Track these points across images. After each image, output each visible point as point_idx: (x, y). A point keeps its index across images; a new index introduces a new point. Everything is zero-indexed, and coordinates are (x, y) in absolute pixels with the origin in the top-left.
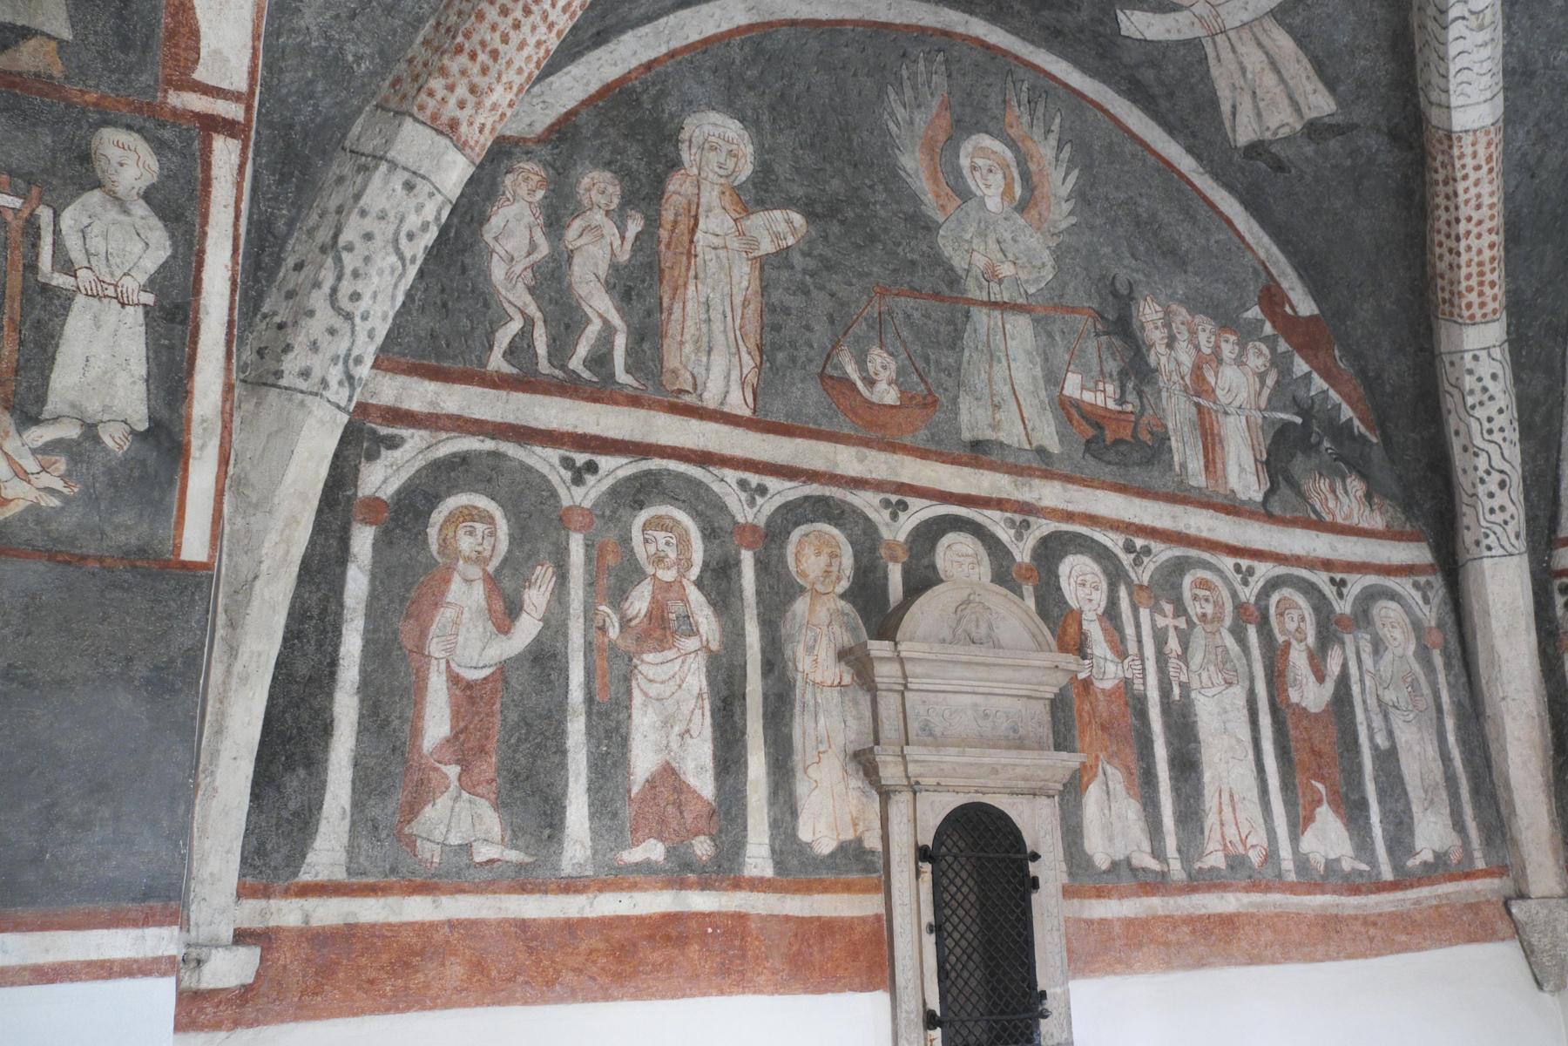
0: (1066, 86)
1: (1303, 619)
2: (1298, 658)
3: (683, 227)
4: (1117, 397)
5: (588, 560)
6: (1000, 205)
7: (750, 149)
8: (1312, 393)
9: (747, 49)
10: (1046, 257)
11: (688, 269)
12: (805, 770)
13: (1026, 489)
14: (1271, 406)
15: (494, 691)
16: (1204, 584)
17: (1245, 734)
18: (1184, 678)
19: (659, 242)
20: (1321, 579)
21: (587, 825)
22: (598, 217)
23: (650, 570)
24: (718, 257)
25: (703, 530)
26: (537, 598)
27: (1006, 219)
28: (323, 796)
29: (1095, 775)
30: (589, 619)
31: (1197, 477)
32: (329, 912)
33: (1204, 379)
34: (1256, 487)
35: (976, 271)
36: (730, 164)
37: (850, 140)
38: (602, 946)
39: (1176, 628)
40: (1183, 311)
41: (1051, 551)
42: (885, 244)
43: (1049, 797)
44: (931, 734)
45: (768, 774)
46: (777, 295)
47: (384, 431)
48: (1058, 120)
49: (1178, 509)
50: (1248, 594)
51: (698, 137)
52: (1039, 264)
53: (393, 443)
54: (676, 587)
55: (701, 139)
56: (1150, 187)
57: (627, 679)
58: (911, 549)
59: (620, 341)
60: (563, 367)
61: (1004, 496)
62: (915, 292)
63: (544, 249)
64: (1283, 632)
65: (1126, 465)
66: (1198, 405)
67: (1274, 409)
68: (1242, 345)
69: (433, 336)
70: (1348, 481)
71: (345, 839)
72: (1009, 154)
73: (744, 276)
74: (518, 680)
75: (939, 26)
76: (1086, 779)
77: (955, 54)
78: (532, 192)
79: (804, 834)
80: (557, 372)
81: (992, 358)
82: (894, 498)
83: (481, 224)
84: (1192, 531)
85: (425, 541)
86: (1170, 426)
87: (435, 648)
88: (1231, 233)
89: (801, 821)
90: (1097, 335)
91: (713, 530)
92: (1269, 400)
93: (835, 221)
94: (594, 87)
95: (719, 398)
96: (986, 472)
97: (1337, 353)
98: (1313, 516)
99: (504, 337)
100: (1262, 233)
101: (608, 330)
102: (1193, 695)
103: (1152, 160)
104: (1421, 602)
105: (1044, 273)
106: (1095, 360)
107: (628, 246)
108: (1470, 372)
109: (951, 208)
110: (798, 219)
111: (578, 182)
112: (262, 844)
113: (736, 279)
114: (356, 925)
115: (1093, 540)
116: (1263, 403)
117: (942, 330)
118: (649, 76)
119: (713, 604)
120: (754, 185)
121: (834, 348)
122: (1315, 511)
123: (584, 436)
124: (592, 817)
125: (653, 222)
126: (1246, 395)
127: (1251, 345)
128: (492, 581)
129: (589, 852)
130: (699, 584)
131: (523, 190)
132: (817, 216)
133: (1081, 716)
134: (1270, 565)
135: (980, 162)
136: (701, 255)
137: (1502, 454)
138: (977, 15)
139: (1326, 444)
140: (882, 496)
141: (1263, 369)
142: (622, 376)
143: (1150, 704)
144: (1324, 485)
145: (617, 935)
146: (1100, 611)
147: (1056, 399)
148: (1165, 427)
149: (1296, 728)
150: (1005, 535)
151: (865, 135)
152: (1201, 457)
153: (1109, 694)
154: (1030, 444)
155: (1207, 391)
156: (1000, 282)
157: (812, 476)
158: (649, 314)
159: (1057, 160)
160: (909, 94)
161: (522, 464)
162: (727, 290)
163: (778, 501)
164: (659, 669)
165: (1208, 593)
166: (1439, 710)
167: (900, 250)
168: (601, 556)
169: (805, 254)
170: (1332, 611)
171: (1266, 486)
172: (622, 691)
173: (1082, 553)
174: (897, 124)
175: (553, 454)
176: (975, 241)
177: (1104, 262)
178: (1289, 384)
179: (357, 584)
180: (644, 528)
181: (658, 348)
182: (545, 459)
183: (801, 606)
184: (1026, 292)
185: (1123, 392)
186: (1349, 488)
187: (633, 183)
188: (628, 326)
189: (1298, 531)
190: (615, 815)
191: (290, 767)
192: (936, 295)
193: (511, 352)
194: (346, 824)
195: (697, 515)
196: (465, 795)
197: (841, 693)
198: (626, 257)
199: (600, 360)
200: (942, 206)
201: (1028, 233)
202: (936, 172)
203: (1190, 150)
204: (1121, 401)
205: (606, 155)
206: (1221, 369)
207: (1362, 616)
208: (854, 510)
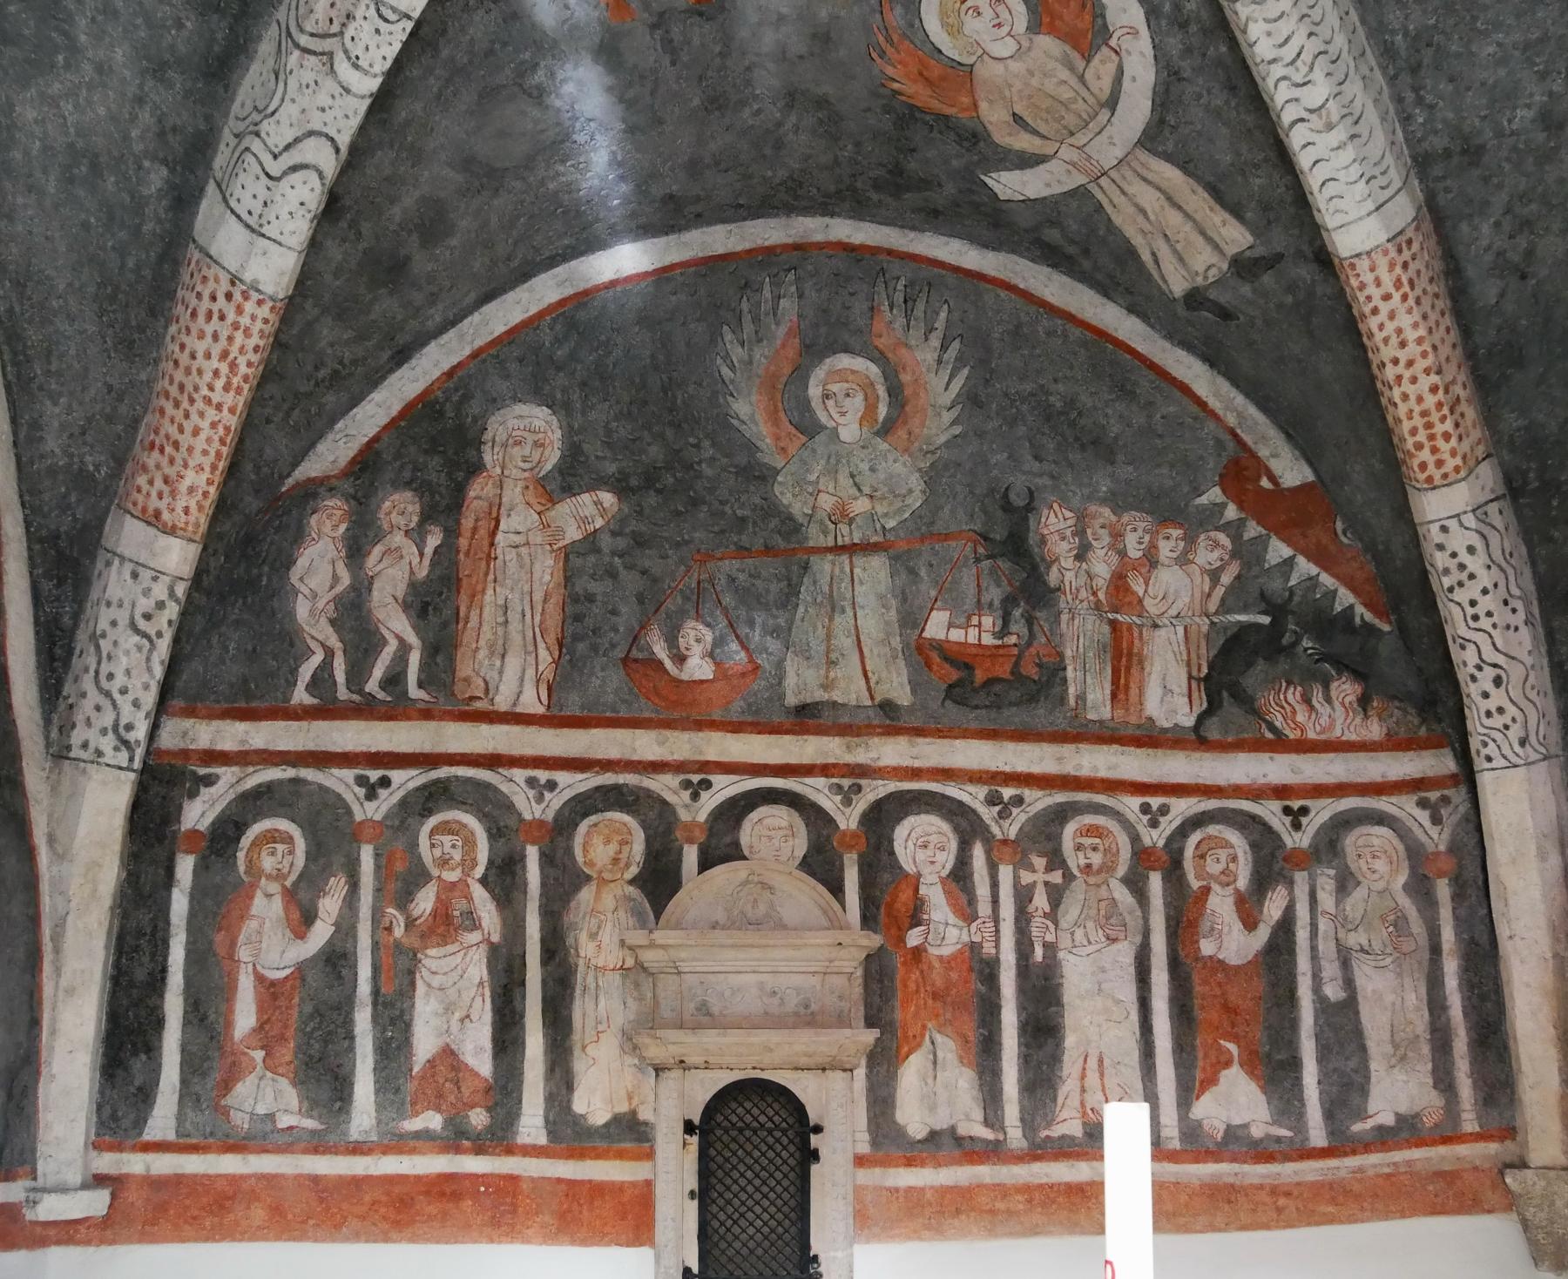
0: (957, 270)
1: (1234, 859)
2: (1221, 905)
3: (483, 533)
5: (378, 867)
7: (558, 434)
8: (1292, 582)
9: (558, 327)
10: (915, 482)
11: (487, 574)
12: (584, 1048)
13: (861, 750)
14: (1224, 608)
15: (293, 988)
16: (1092, 831)
17: (1129, 993)
18: (1050, 938)
19: (458, 552)
20: (1270, 811)
21: (372, 1098)
22: (398, 539)
23: (435, 872)
24: (519, 555)
25: (488, 831)
26: (330, 905)
28: (159, 1075)
29: (919, 1045)
30: (376, 920)
31: (1099, 704)
32: (164, 1164)
33: (1128, 589)
35: (821, 515)
36: (536, 456)
37: (675, 397)
38: (384, 1198)
39: (1046, 884)
40: (1106, 512)
41: (882, 817)
42: (710, 505)
43: (845, 1070)
44: (709, 1014)
45: (546, 1053)
46: (583, 584)
47: (202, 771)
48: (943, 315)
49: (1067, 749)
50: (1155, 838)
51: (501, 437)
53: (209, 781)
54: (460, 886)
55: (505, 436)
56: (1071, 368)
57: (411, 973)
58: (711, 829)
59: (415, 659)
60: (361, 692)
61: (831, 760)
62: (743, 552)
63: (346, 580)
64: (1197, 877)
66: (1114, 624)
67: (1228, 612)
68: (1190, 540)
69: (245, 681)
70: (1334, 685)
71: (175, 1108)
72: (873, 370)
73: (546, 570)
74: (314, 978)
75: (790, 241)
76: (906, 1049)
77: (810, 268)
79: (579, 1106)
80: (356, 697)
81: (833, 610)
82: (696, 778)
84: (1085, 772)
85: (235, 863)
86: (1068, 653)
87: (243, 954)
88: (1186, 401)
89: (576, 1095)
90: (978, 560)
91: (499, 829)
92: (1223, 600)
93: (652, 493)
94: (396, 408)
95: (510, 701)
96: (811, 738)
97: (1339, 526)
98: (1269, 735)
99: (306, 672)
101: (404, 647)
102: (1061, 955)
103: (1076, 332)
104: (1427, 823)
105: (909, 501)
106: (972, 590)
107: (427, 562)
108: (1441, 547)
109: (792, 450)
110: (608, 498)
111: (379, 507)
112: (114, 1112)
113: (536, 576)
114: (183, 1175)
115: (944, 796)
116: (1213, 606)
118: (451, 384)
119: (495, 897)
120: (561, 472)
121: (642, 628)
122: (1272, 727)
123: (377, 754)
124: (377, 1092)
125: (452, 533)
126: (1187, 600)
127: (1202, 537)
128: (290, 895)
129: (374, 1122)
130: (484, 881)
131: (327, 528)
133: (905, 986)
134: (1192, 800)
135: (835, 388)
136: (501, 557)
137: (1494, 644)
138: (839, 216)
139: (1306, 643)
140: (682, 777)
141: (1219, 564)
142: (414, 692)
143: (1003, 966)
144: (1293, 695)
145: (397, 1190)
146: (945, 873)
147: (913, 644)
148: (1061, 655)
149: (1205, 982)
150: (829, 802)
151: (691, 389)
153: (948, 962)
154: (872, 698)
155: (1130, 603)
156: (851, 521)
157: (607, 765)
158: (445, 625)
159: (940, 362)
160: (748, 328)
161: (321, 787)
162: (527, 588)
163: (568, 795)
164: (443, 962)
165: (1097, 841)
166: (1436, 949)
168: (390, 860)
169: (614, 534)
170: (1282, 845)
171: (1201, 705)
172: (406, 982)
173: (927, 812)
174: (732, 368)
175: (349, 774)
176: (822, 480)
177: (995, 472)
178: (1257, 577)
179: (179, 904)
180: (432, 834)
181: (451, 660)
182: (340, 780)
183: (586, 895)
186: (1333, 694)
187: (432, 496)
189: (1242, 757)
190: (397, 1090)
191: (135, 1054)
192: (768, 550)
193: (314, 685)
194: (176, 1097)
195: (483, 817)
196: (269, 1074)
197: (624, 977)
198: (424, 573)
199: (394, 680)
201: (891, 458)
202: (776, 411)
203: (1131, 310)
204: (1003, 632)
205: (407, 474)
207: (1329, 845)
208: (649, 794)
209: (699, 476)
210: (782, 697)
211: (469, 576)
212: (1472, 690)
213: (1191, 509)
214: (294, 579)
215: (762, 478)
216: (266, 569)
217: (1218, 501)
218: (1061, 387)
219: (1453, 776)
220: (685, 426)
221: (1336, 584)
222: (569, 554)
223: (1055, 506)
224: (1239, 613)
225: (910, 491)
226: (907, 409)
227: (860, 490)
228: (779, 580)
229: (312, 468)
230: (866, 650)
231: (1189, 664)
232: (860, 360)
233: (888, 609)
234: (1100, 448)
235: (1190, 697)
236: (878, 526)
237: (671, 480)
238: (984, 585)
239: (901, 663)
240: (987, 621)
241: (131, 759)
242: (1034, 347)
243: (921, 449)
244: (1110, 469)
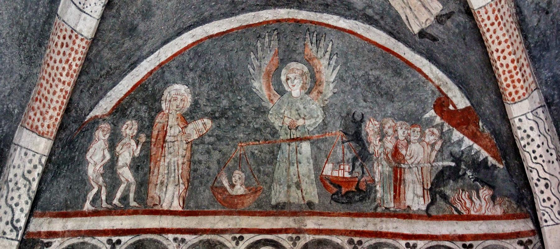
3: (161, 136)
34: (423, 203)
37: (232, 82)
52: (316, 116)
59: (133, 188)
63: (108, 157)
78: (104, 135)
83: (86, 153)
90: (343, 143)
93: (224, 119)
97: (481, 124)
105: (317, 120)
117: (267, 156)
125: (149, 136)
126: (422, 157)
132: (216, 118)
141: (433, 141)
152: (392, 192)
158: (145, 174)
167: (251, 125)
174: (254, 69)
176: (286, 113)
178: (449, 146)
188: (136, 182)
209: (241, 111)
211: (154, 154)
212: (536, 190)
213: (423, 119)
214: (88, 157)
216: (77, 153)
219: (532, 231)
220: (236, 92)
221: (481, 148)
222: (192, 144)
225: (318, 116)
227: (300, 116)
228: (270, 153)
229: (97, 112)
231: (423, 184)
232: (300, 64)
234: (390, 97)
236: (306, 130)
237: (231, 114)
238: (345, 152)
241: (17, 235)
244: (392, 104)
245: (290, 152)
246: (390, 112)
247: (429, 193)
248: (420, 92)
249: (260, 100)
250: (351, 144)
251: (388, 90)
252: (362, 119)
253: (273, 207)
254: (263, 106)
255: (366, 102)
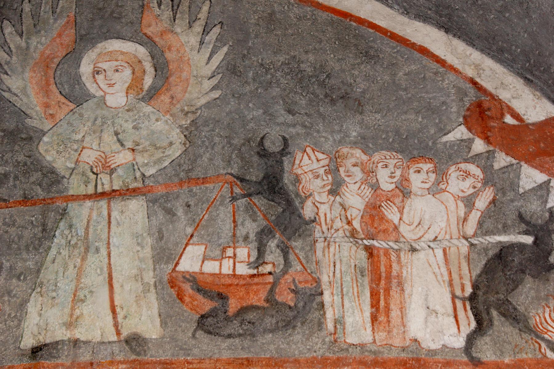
4: (252, 259)
6: (126, 99)
10: (177, 136)
27: (128, 111)
33: (382, 218)
40: (358, 153)
48: (205, 8)
52: (165, 144)
56: (320, 42)
65: (253, 335)
66: (370, 251)
67: (488, 233)
72: (141, 51)
88: (425, 60)
90: (234, 199)
92: (480, 224)
100: (470, 50)
103: (325, 15)
106: (228, 226)
109: (60, 115)
126: (443, 225)
127: (453, 168)
141: (472, 191)
147: (166, 278)
148: (318, 281)
154: (118, 333)
155: (385, 231)
156: (112, 171)
159: (202, 43)
176: (87, 139)
178: (512, 201)
184: (144, 175)
185: (261, 251)
192: (26, 200)
200: (51, 115)
201: (153, 118)
202: (48, 84)
206: (408, 202)
210: (19, 338)
215: (30, 139)
217: (465, 137)
218: (311, 57)
223: (309, 150)
224: (499, 233)
226: (171, 79)
227: (122, 145)
230: (116, 286)
231: (451, 284)
232: (130, 44)
233: (142, 247)
235: (456, 317)
236: (138, 174)
238: (239, 220)
239: (152, 297)
240: (242, 252)
242: (286, 29)
243: (182, 110)
244: (358, 117)
245: (91, 222)
246: (354, 134)
247: (468, 308)
248: (427, 92)
249: (23, 114)
250: (256, 201)
251: (349, 91)
252: (283, 149)
253: (23, 355)
254: (26, 128)
255: (293, 115)
